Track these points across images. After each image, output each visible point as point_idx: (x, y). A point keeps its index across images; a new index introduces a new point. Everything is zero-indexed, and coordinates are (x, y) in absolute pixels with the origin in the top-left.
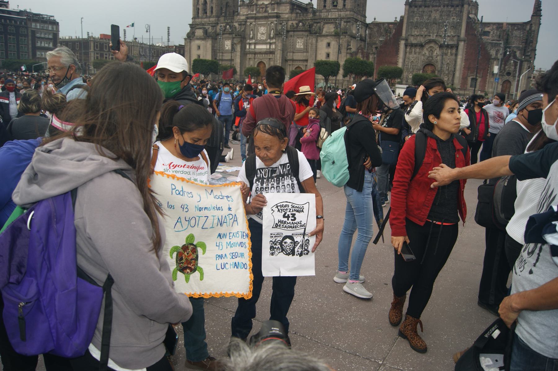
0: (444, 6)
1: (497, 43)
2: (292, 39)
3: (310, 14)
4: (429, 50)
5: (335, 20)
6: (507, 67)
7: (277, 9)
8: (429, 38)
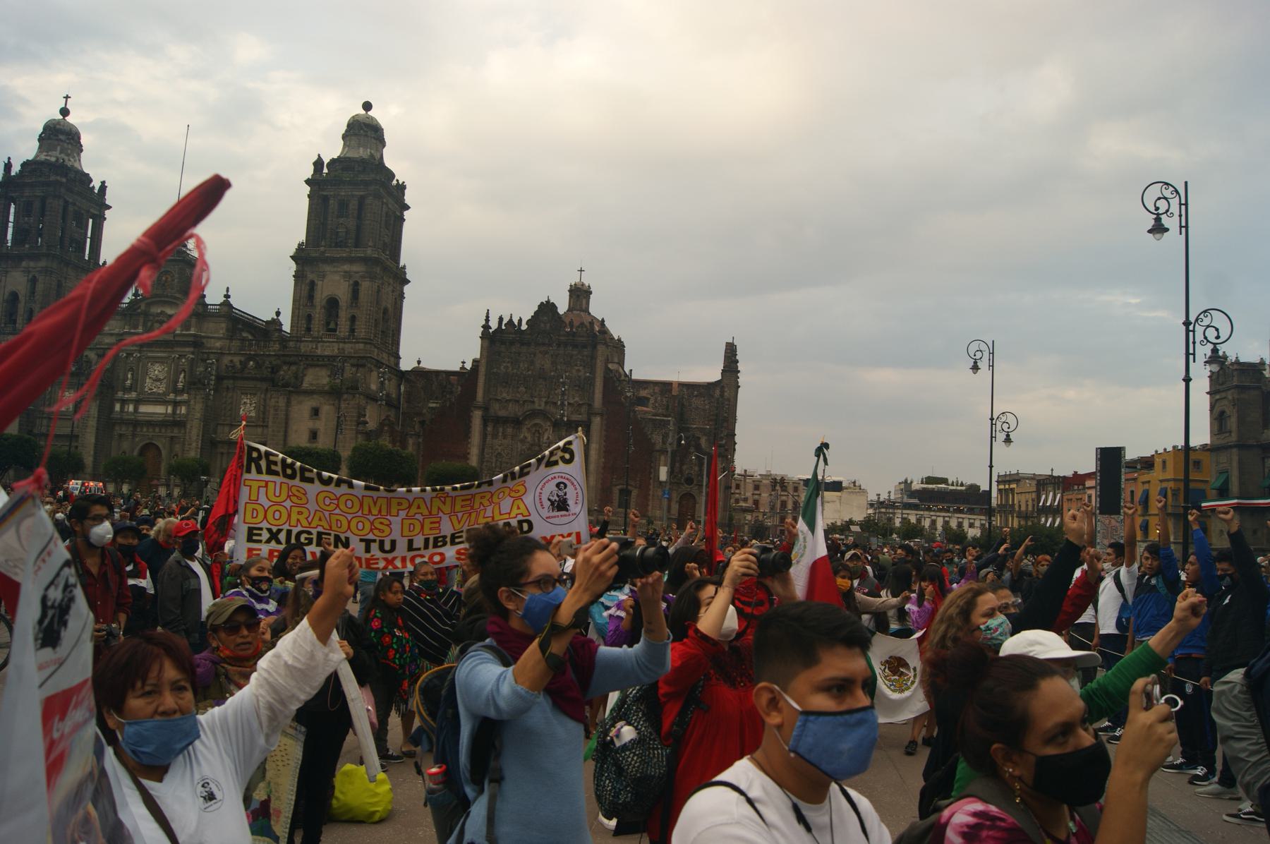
0: (559, 345)
1: (663, 420)
2: (230, 395)
4: (533, 431)
5: (331, 359)
6: (685, 467)
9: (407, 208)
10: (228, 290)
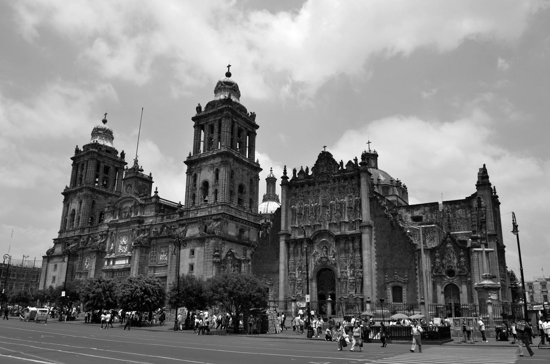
1: (428, 227)
6: (444, 262)
7: (141, 212)
9: (257, 127)
10: (157, 188)
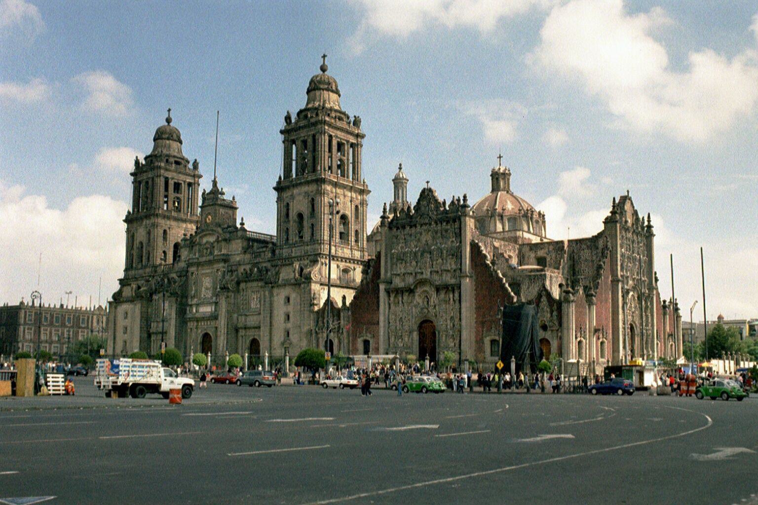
3: (268, 253)
8: (419, 277)
